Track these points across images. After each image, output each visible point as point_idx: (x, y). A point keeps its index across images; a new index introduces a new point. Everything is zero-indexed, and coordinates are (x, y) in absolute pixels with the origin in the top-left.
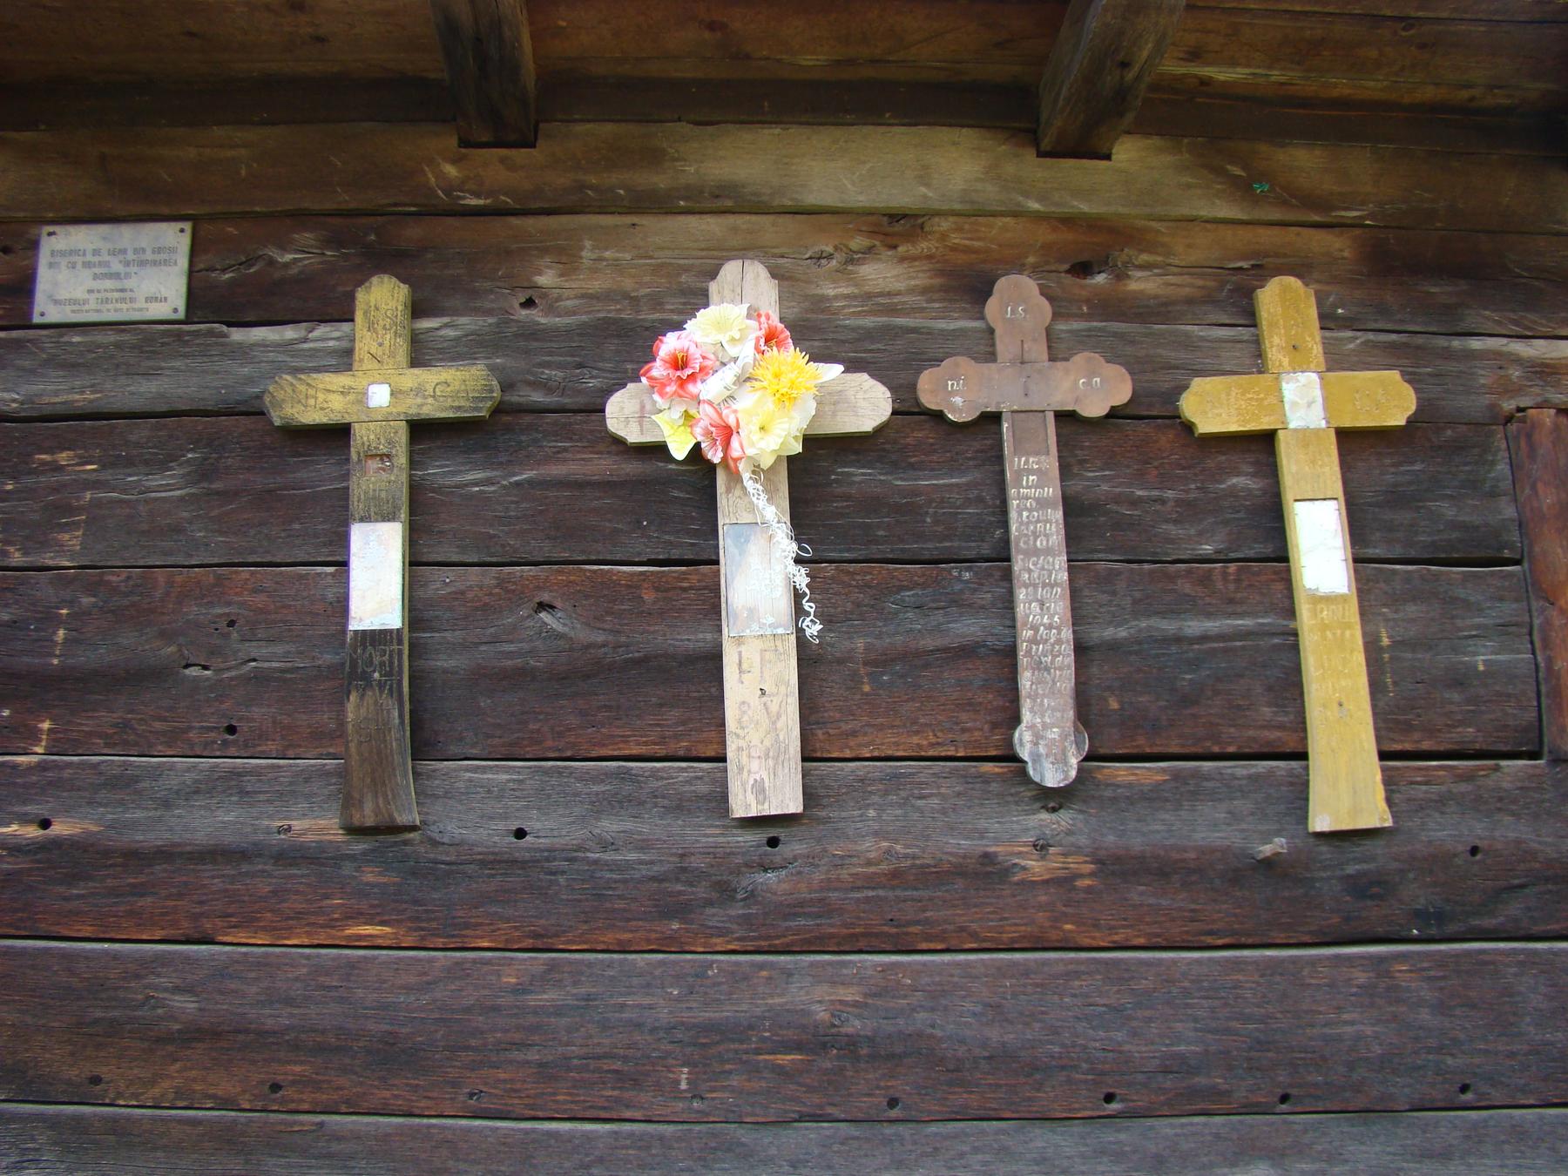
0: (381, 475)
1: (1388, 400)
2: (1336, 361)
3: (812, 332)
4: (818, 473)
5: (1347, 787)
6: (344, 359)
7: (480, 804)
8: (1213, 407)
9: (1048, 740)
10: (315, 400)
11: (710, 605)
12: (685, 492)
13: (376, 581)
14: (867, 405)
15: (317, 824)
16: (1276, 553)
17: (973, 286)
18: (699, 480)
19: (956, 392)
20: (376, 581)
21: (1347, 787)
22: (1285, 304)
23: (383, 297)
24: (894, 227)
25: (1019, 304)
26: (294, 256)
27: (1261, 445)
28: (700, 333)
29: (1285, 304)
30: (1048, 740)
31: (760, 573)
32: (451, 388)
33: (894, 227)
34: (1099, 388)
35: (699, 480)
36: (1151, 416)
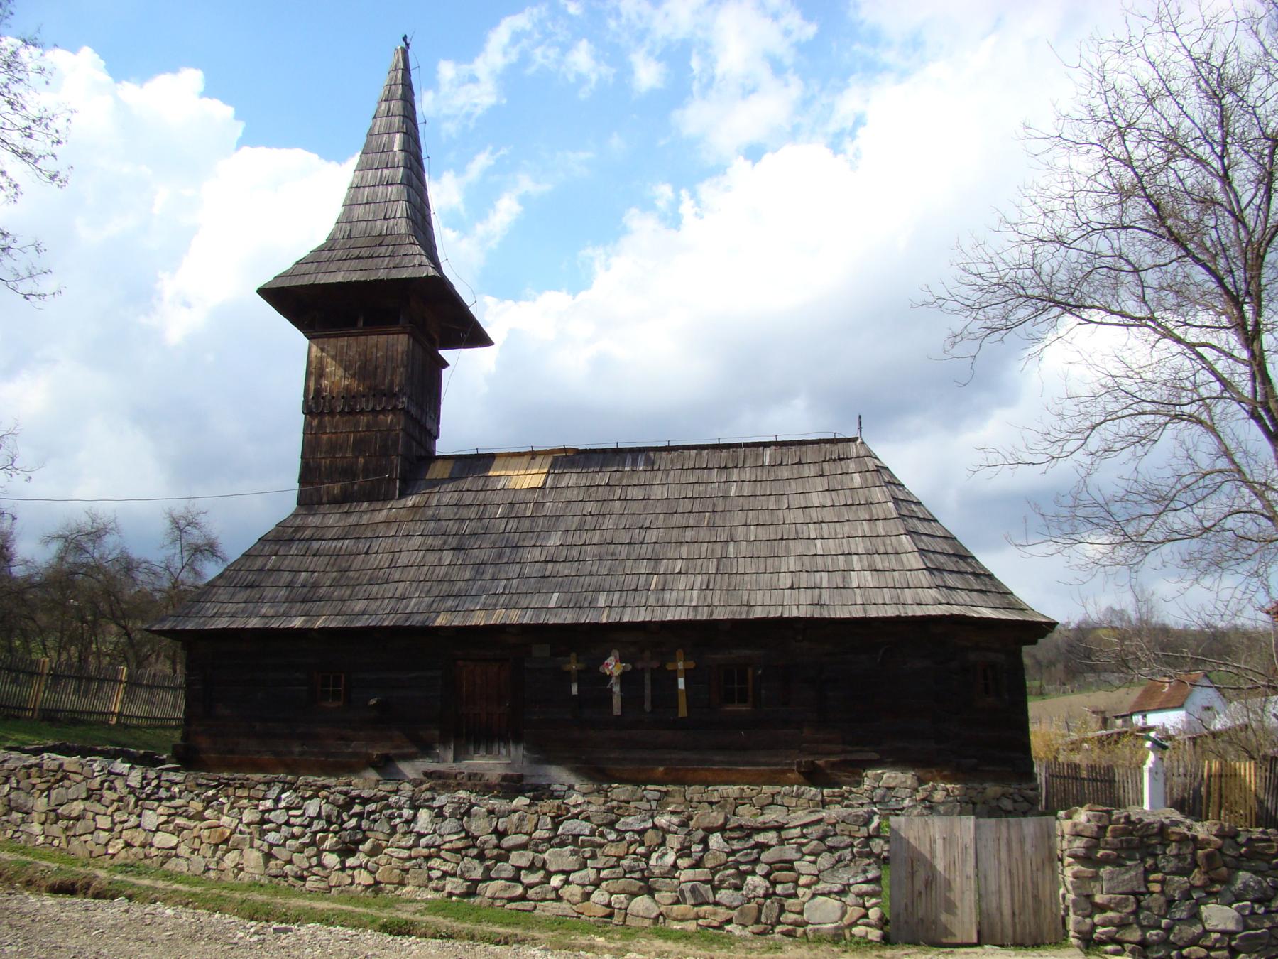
1: (691, 665)
2: (685, 661)
3: (621, 660)
4: (623, 677)
5: (683, 712)
6: (569, 663)
8: (670, 667)
9: (647, 706)
10: (567, 667)
13: (575, 689)
14: (629, 667)
18: (610, 677)
19: (639, 665)
20: (575, 689)
21: (683, 712)
22: (680, 653)
23: (573, 655)
25: (647, 654)
27: (675, 671)
28: (608, 661)
29: (680, 653)
30: (647, 706)
31: (616, 689)
32: (581, 666)
34: (655, 664)
35: (610, 677)
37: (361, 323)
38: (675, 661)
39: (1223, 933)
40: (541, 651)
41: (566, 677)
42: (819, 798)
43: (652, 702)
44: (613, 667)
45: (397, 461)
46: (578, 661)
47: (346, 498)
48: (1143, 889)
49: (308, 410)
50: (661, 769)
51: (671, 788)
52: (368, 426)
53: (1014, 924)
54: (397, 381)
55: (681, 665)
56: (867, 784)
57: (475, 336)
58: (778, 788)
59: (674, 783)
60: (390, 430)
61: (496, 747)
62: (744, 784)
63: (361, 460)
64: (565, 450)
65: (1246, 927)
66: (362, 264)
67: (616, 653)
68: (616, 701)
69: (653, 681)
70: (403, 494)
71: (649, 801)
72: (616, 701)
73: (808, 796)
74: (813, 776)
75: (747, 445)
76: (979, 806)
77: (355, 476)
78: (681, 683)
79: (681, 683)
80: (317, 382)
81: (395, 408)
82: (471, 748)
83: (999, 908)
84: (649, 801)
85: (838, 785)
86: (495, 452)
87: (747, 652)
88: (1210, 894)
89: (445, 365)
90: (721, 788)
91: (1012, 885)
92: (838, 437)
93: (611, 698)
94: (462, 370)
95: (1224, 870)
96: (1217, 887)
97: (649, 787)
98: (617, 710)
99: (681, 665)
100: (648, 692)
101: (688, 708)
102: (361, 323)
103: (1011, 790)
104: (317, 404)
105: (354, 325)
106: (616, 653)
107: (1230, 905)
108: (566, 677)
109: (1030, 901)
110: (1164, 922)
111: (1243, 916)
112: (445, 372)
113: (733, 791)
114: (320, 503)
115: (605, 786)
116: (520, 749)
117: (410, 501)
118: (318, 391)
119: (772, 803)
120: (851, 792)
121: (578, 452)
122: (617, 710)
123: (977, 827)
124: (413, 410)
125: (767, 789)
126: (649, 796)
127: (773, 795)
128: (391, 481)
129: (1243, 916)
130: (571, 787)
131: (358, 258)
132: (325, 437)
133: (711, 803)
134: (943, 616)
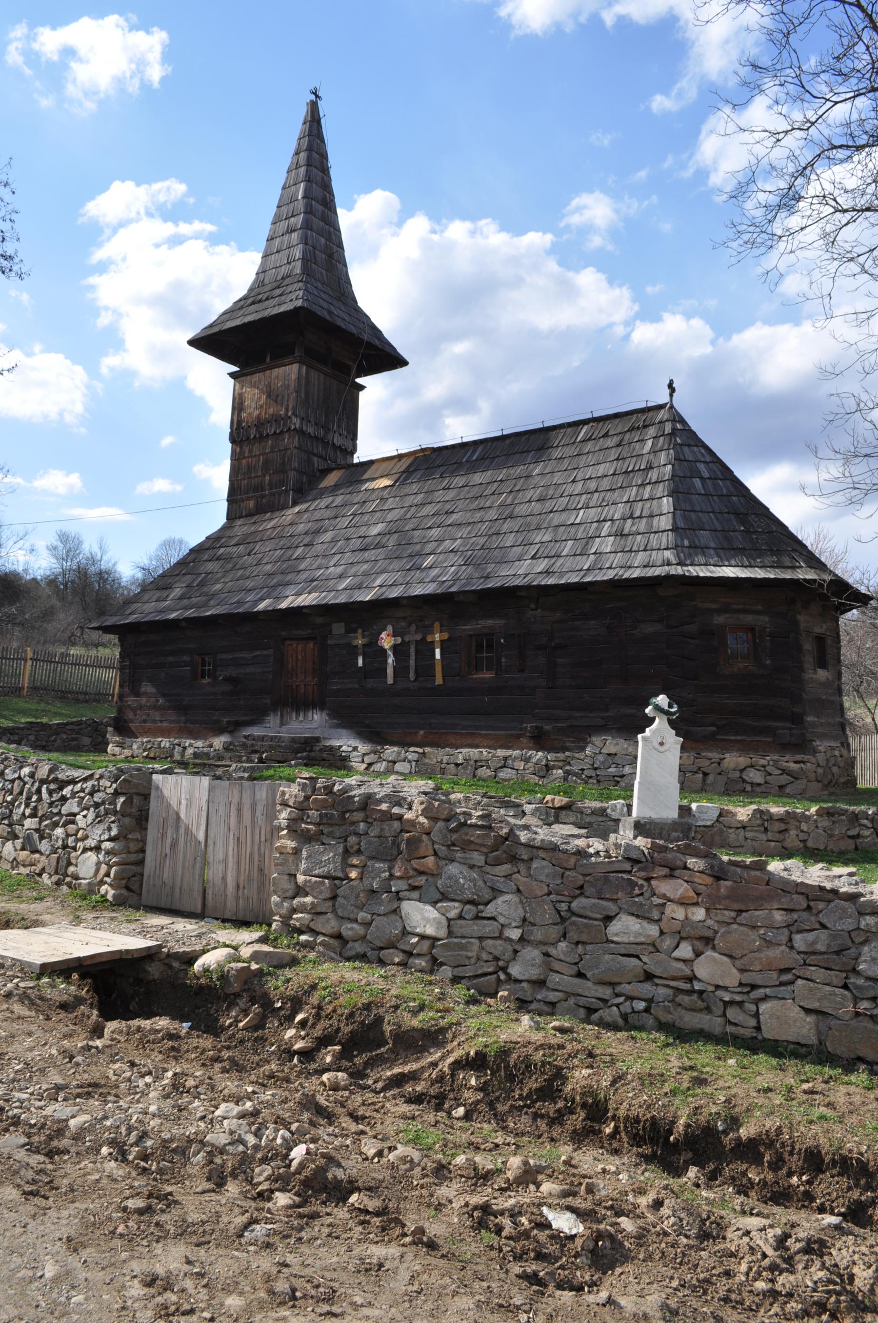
0: (360, 651)
1: (446, 636)
4: (395, 648)
5: (439, 680)
7: (370, 683)
8: (429, 639)
9: (412, 676)
10: (355, 643)
11: (386, 662)
14: (399, 640)
15: (357, 686)
16: (434, 655)
17: (409, 625)
19: (407, 639)
21: (439, 680)
22: (437, 625)
23: (360, 631)
24: (404, 618)
25: (413, 627)
26: (353, 626)
29: (437, 625)
31: (391, 660)
32: (365, 640)
33: (404, 618)
34: (418, 637)
36: (424, 639)
37: (268, 360)
38: (433, 633)
39: (423, 937)
40: (338, 628)
41: (353, 651)
42: (544, 763)
43: (416, 672)
44: (387, 641)
45: (292, 474)
46: (363, 637)
47: (260, 510)
48: (340, 875)
49: (233, 439)
50: (422, 732)
51: (427, 750)
52: (272, 447)
53: (237, 898)
54: (291, 406)
55: (437, 637)
56: (588, 751)
57: (386, 359)
58: (510, 752)
59: (431, 745)
60: (286, 450)
61: (310, 714)
62: (484, 747)
63: (267, 478)
64: (423, 450)
65: (450, 934)
66: (253, 308)
67: (390, 628)
68: (390, 671)
69: (417, 651)
70: (295, 504)
71: (410, 762)
72: (390, 671)
73: (534, 760)
74: (540, 741)
75: (570, 425)
76: (711, 778)
77: (263, 490)
78: (438, 652)
80: (239, 415)
81: (289, 430)
82: (294, 715)
83: (224, 878)
84: (410, 762)
85: (564, 749)
86: (373, 458)
87: (490, 622)
88: (414, 888)
89: (362, 388)
90: (464, 750)
91: (239, 855)
92: (650, 404)
94: (375, 391)
95: (430, 861)
96: (421, 880)
97: (412, 749)
98: (390, 680)
100: (412, 662)
102: (268, 360)
103: (763, 762)
104: (238, 434)
105: (264, 361)
106: (390, 628)
107: (434, 904)
108: (353, 651)
109: (255, 874)
110: (362, 915)
111: (449, 920)
112: (362, 395)
114: (241, 517)
116: (324, 715)
117: (297, 509)
118: (239, 422)
119: (504, 766)
120: (573, 758)
121: (434, 450)
122: (390, 680)
123: (211, 789)
124: (311, 430)
125: (501, 753)
126: (410, 757)
127: (505, 759)
128: (287, 491)
129: (449, 920)
130: (355, 749)
131: (260, 301)
132: (244, 461)
133: (457, 765)
134: (658, 577)
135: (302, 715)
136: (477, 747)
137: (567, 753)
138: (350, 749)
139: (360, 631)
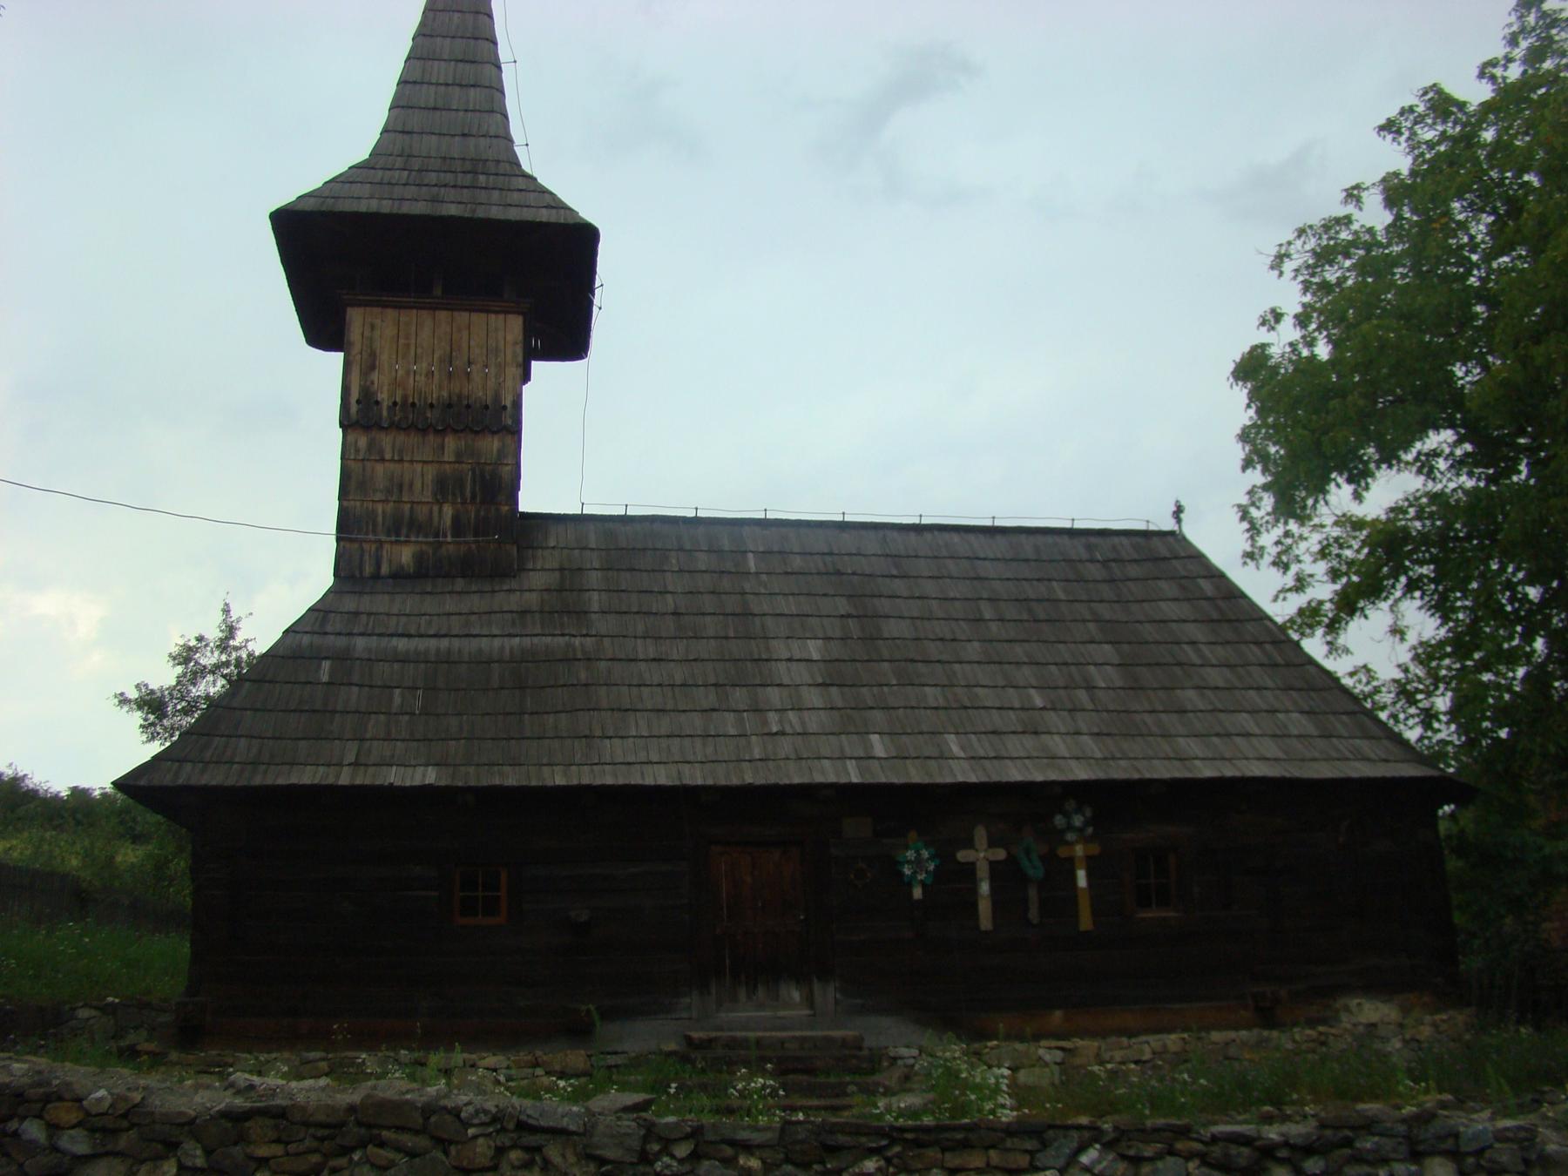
1: (1095, 849)
5: (1086, 922)
6: (907, 848)
8: (1062, 852)
9: (1033, 914)
11: (974, 891)
12: (969, 870)
21: (1086, 922)
23: (913, 835)
30: (1033, 914)
31: (985, 888)
44: (981, 854)
51: (1079, 1042)
55: (1079, 850)
56: (1346, 1021)
58: (1232, 1034)
68: (984, 907)
72: (984, 907)
78: (1082, 879)
79: (1082, 879)
82: (742, 994)
93: (974, 906)
97: (1043, 1043)
98: (985, 921)
99: (1079, 850)
101: (1095, 913)
113: (1173, 1040)
115: (977, 1045)
122: (985, 921)
127: (1227, 1044)
135: (761, 992)
136: (1170, 1031)
137: (1321, 1029)
138: (915, 1052)
139: (913, 835)
